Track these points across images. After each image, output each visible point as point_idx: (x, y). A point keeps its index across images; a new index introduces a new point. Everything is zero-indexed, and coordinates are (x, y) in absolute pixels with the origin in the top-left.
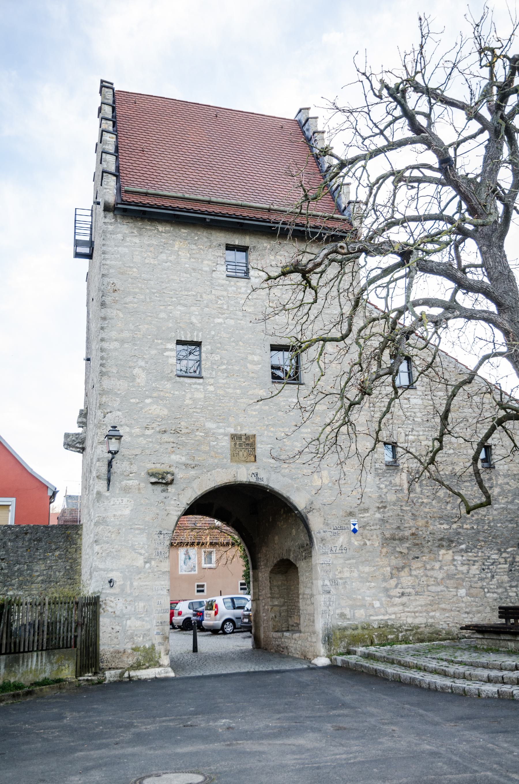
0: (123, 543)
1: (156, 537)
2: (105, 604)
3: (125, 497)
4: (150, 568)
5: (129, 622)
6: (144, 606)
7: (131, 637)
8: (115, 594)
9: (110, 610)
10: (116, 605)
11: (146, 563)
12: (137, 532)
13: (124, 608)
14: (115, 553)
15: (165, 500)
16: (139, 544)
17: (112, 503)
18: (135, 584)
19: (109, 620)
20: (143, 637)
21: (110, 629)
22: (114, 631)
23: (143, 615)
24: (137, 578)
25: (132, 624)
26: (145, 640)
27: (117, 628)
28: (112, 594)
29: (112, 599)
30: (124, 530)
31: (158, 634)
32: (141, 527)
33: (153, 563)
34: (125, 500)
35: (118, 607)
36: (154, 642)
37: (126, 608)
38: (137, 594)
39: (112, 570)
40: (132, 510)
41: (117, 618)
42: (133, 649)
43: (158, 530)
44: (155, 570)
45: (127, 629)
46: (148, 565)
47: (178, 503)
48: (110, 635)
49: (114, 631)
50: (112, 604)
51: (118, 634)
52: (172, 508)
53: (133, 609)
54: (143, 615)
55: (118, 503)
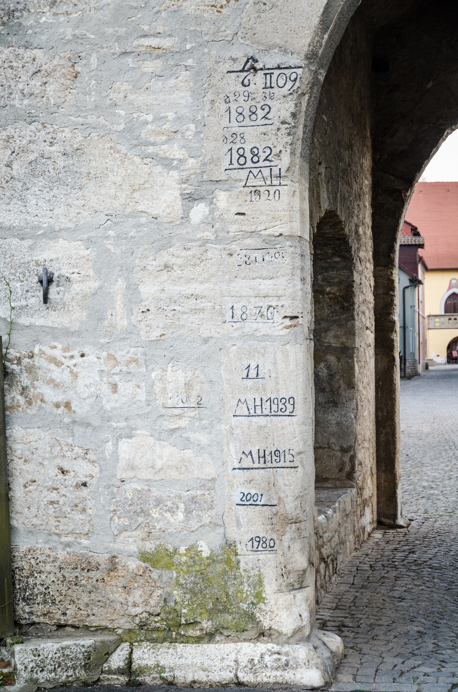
0: (92, 119)
1: (232, 84)
2: (30, 370)
4: (209, 222)
5: (125, 447)
6: (188, 385)
7: (139, 509)
9: (51, 395)
10: (75, 376)
11: (190, 199)
13: (106, 389)
16: (158, 119)
18: (148, 290)
19: (46, 436)
20: (188, 512)
22: (70, 480)
23: (182, 423)
24: (153, 264)
25: (142, 456)
26: (194, 524)
27: (82, 469)
28: (54, 333)
29: (57, 353)
31: (248, 500)
33: (222, 199)
35: (81, 382)
36: (233, 534)
37: (115, 388)
39: (52, 234)
41: (79, 430)
42: (144, 557)
43: (240, 53)
44: (233, 228)
45: (120, 475)
46: (199, 211)
48: (54, 496)
49: (70, 480)
50: (56, 373)
51: (85, 492)
53: (142, 396)
54: (182, 423)
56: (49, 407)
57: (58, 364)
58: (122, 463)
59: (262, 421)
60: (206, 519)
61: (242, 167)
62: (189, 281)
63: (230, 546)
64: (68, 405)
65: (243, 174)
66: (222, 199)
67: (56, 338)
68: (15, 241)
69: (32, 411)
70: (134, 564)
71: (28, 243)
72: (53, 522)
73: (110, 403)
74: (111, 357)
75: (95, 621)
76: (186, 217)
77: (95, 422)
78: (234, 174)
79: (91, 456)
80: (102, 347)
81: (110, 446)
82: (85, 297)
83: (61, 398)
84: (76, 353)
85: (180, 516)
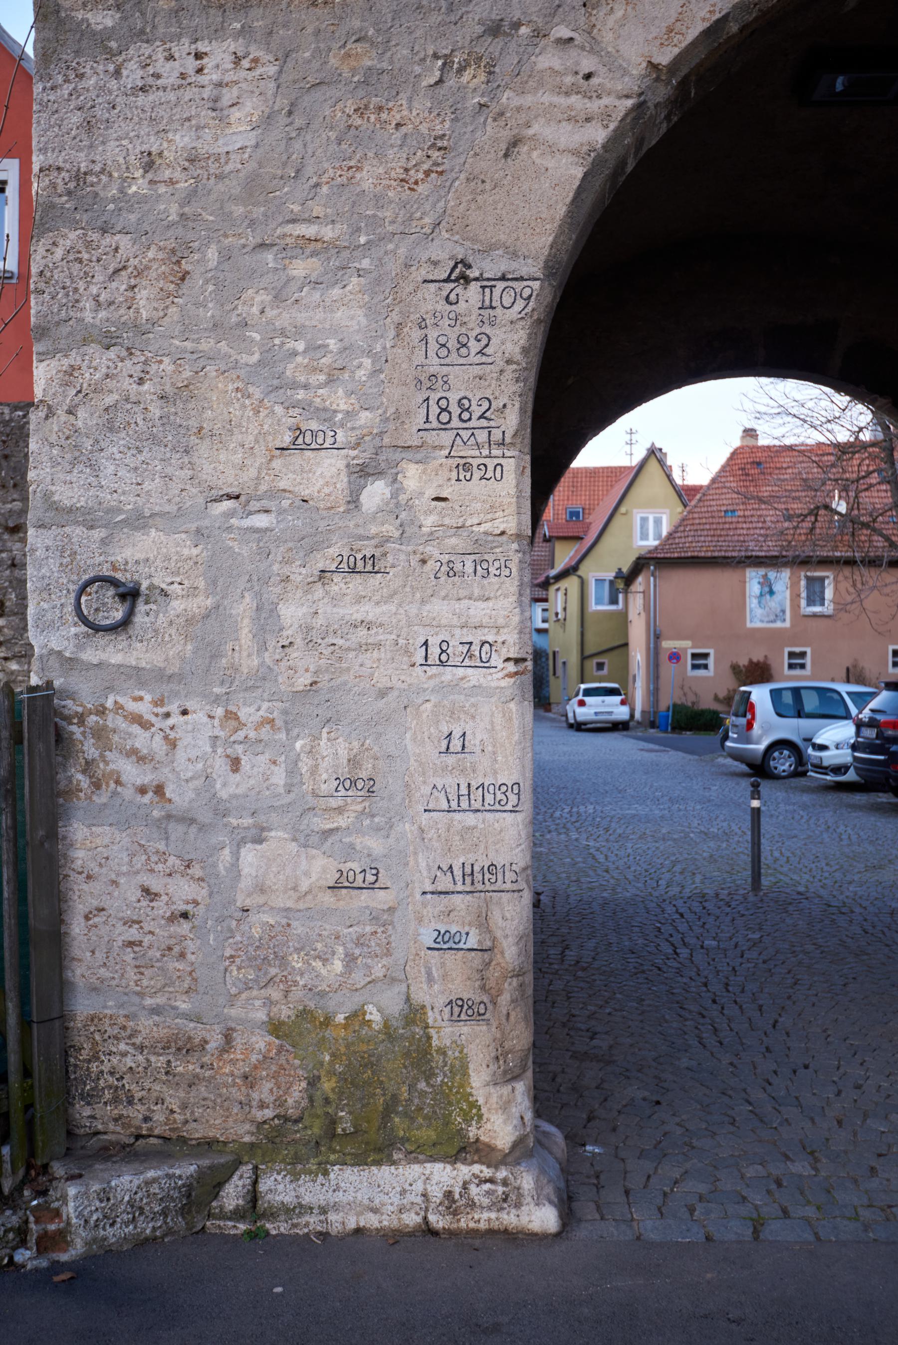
2: (100, 734)
3: (218, 33)
5: (250, 858)
6: (354, 762)
8: (162, 676)
11: (363, 473)
12: (300, 268)
13: (220, 765)
14: (156, 411)
15: (495, 46)
17: (133, 75)
18: (292, 613)
20: (350, 960)
21: (134, 894)
22: (161, 908)
23: (341, 821)
24: (299, 574)
25: (276, 871)
26: (359, 978)
27: (182, 891)
28: (137, 675)
29: (144, 708)
30: (212, 254)
31: (445, 942)
32: (328, 233)
33: (412, 476)
34: (219, 53)
35: (181, 755)
36: (422, 994)
37: (235, 764)
38: (302, 681)
39: (139, 521)
40: (268, 119)
41: (176, 830)
43: (444, 250)
44: (429, 522)
46: (376, 493)
47: (587, 64)
48: (133, 933)
49: (161, 908)
50: (141, 739)
51: (185, 927)
52: (547, 98)
53: (279, 777)
54: (341, 821)
55: (170, 76)
56: (128, 793)
57: (145, 725)
58: (245, 883)
59: (470, 819)
60: (378, 971)
61: (444, 427)
62: (359, 599)
63: (414, 1014)
64: (159, 790)
65: (446, 438)
66: (412, 476)
67: (142, 684)
68: (78, 531)
69: (101, 798)
70: (261, 1041)
71: (98, 534)
72: (131, 974)
73: (229, 786)
74: (230, 715)
75: (198, 1132)
76: (354, 501)
77: (204, 816)
78: (431, 438)
79: (196, 870)
80: (217, 700)
81: (226, 854)
82: (190, 621)
83: (148, 778)
84: (174, 708)
85: (338, 966)
